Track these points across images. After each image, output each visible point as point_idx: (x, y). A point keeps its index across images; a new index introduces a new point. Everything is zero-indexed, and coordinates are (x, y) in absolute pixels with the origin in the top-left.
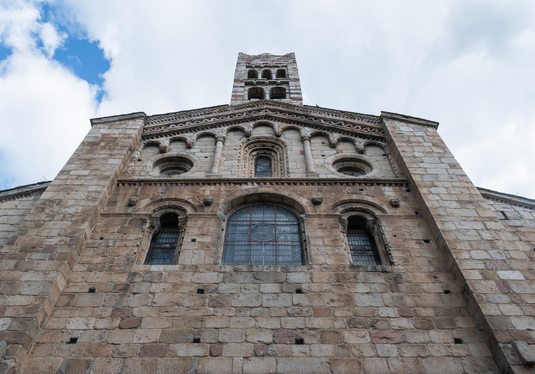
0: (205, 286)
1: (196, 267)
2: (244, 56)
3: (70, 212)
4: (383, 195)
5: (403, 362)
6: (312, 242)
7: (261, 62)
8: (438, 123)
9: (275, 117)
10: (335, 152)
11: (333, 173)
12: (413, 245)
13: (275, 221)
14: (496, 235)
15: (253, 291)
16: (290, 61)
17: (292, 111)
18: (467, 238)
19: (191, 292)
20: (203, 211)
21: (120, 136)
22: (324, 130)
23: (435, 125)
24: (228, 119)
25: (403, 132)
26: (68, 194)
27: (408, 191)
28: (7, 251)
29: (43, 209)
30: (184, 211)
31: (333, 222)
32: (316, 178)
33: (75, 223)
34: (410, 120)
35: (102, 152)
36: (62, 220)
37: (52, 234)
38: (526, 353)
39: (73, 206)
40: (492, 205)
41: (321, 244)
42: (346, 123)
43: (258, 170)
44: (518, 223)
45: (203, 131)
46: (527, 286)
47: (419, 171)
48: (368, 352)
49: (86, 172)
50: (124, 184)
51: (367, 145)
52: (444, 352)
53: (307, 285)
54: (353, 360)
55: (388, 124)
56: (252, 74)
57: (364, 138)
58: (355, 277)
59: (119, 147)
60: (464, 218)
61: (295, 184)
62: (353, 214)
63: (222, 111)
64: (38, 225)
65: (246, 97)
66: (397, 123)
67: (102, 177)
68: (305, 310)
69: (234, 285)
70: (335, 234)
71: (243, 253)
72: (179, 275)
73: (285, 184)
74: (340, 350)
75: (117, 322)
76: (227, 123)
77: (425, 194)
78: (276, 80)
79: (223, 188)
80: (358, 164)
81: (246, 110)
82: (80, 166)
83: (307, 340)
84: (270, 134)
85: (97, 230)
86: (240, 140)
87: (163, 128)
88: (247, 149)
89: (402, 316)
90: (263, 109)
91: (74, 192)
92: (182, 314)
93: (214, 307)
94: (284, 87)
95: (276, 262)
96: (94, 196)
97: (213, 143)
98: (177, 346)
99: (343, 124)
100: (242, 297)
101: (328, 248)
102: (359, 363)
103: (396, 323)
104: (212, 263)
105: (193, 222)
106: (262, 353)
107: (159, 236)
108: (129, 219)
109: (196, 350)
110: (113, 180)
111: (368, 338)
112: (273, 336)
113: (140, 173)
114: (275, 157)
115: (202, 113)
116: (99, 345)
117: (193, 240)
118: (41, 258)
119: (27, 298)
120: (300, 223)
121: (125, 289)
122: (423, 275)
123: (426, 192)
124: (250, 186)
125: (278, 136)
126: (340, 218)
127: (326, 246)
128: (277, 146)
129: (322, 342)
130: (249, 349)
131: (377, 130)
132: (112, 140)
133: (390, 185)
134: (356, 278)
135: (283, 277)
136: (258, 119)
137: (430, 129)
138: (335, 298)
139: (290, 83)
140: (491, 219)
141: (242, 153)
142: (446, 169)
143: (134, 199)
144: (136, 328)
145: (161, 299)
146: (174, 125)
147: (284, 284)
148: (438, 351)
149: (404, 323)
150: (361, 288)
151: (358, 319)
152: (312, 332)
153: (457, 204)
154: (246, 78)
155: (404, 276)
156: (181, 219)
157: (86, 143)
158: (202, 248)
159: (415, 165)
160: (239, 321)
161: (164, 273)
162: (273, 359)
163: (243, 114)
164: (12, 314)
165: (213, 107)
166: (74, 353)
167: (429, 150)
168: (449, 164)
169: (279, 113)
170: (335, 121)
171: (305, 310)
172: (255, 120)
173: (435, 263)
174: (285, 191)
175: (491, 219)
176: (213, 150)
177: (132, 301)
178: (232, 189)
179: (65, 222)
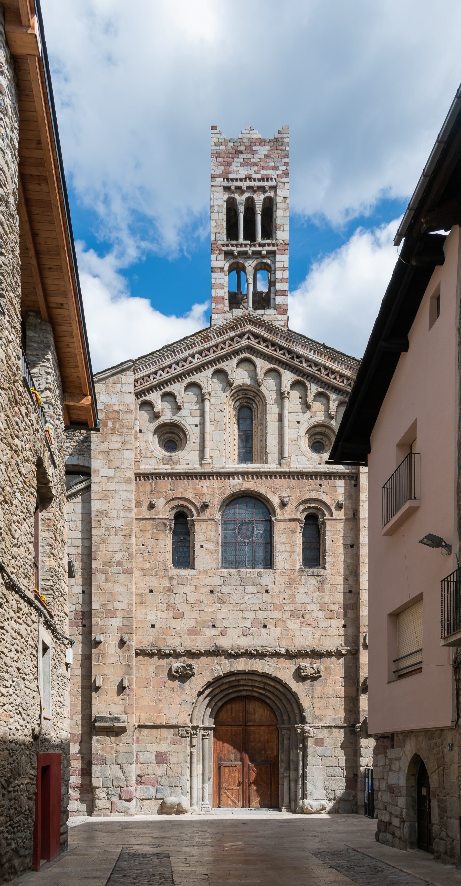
0: (214, 588)
1: (207, 572)
65: (225, 239)
69: (230, 587)
75: (171, 615)
95: (253, 546)
104: (216, 568)
121: (169, 590)
132: (116, 416)
145: (192, 598)
177: (175, 599)
178: (223, 485)
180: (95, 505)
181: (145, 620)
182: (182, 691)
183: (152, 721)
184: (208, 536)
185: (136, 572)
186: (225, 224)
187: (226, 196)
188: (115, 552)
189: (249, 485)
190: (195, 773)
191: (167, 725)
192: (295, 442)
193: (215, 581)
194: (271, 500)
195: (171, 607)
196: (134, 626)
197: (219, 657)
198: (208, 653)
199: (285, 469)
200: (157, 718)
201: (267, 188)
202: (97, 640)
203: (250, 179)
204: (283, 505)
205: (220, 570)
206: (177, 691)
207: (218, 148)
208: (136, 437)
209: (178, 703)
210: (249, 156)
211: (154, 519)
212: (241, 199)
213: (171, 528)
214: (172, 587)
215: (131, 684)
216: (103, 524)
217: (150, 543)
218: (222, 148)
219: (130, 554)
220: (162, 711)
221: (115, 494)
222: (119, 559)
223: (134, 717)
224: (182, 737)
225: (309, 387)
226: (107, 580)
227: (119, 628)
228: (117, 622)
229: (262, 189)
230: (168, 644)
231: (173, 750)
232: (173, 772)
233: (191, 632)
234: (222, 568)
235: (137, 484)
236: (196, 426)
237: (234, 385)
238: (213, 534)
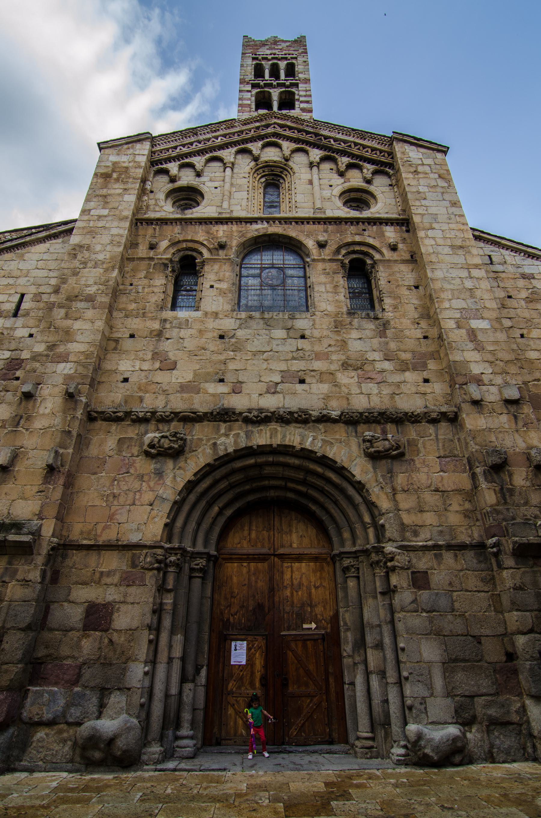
0: (225, 332)
2: (249, 42)
3: (100, 259)
4: (384, 236)
5: (381, 397)
6: (316, 288)
7: (269, 52)
8: (448, 148)
9: (283, 135)
10: (341, 180)
11: (339, 208)
12: (404, 292)
13: (284, 264)
14: (477, 283)
15: (264, 336)
16: (300, 51)
17: (301, 127)
18: (451, 287)
19: (214, 337)
20: (218, 255)
21: (131, 164)
22: (333, 153)
23: (444, 150)
24: (236, 138)
25: (412, 160)
26: (94, 238)
27: (408, 231)
28: (55, 300)
29: (75, 256)
30: (201, 253)
31: (335, 267)
32: (323, 216)
33: (106, 270)
34: (420, 143)
35: (116, 186)
36: (94, 268)
37: (89, 283)
38: (475, 393)
39: (100, 251)
40: (481, 248)
41: (324, 290)
42: (356, 144)
43: (267, 200)
44: (500, 268)
45: (211, 155)
46: (491, 334)
47: (420, 211)
48: (355, 390)
49: (105, 212)
50: (142, 223)
51: (375, 173)
52: (414, 390)
53: (310, 331)
54: (343, 397)
55: (398, 147)
56: (259, 71)
57: (373, 164)
58: (350, 323)
59: (131, 180)
60: (453, 266)
61: (303, 223)
62: (354, 256)
63: (229, 128)
64: (75, 273)
66: (407, 147)
67: (121, 217)
69: (249, 331)
70: (336, 279)
71: (256, 298)
72: (202, 321)
73: (293, 223)
74: (334, 389)
75: (157, 365)
76: (235, 143)
77: (422, 238)
79: (235, 228)
80: (364, 196)
82: (98, 203)
83: (308, 380)
84: (278, 156)
85: (126, 275)
86: (248, 165)
87: (170, 150)
88: (255, 175)
89: (386, 360)
90: (272, 124)
91: (100, 236)
92: (208, 358)
93: (233, 351)
94: (293, 90)
96: (118, 240)
97: (222, 169)
98: (207, 385)
99: (353, 146)
100: (256, 342)
101: (330, 294)
102: (348, 399)
103: (379, 366)
104: (230, 310)
105: (210, 267)
106: (273, 390)
107: (180, 279)
108: (153, 263)
109: (222, 388)
110: (132, 220)
112: (282, 377)
113: (154, 208)
114: (283, 185)
115: (209, 130)
116: (147, 384)
117: (212, 287)
118: (85, 307)
119: (83, 345)
120: (304, 267)
121: (159, 334)
122: (408, 321)
123: (424, 236)
124: (259, 226)
125: (287, 160)
126: (342, 263)
127: (328, 292)
128: (286, 173)
129: (321, 382)
130: (262, 387)
131: (386, 155)
133: (392, 224)
134: (352, 325)
135: (289, 324)
136: (267, 138)
137: (439, 155)
138: (333, 343)
139: (300, 85)
140: (476, 266)
141: (251, 182)
142: (447, 208)
143: (154, 241)
144: (173, 369)
145: (190, 344)
146: (181, 147)
147: (291, 331)
149: (387, 365)
151: (350, 362)
152: (312, 373)
153: (449, 249)
154: (253, 79)
155: (392, 323)
156: (199, 262)
157: (99, 174)
158: (220, 294)
159: (417, 203)
160: (254, 364)
161: (190, 320)
162: (281, 396)
163: (250, 131)
164: (75, 360)
165: (220, 123)
166: (128, 390)
167: (433, 183)
168: (450, 201)
169: (287, 129)
170: (345, 142)
172: (263, 139)
173: (420, 310)
174: (292, 231)
175: (476, 266)
176: (222, 178)
177: (166, 346)
178: (243, 229)
179: (98, 269)
182: (159, 480)
184: (221, 276)
190: (163, 656)
191: (120, 543)
194: (304, 242)
197: (228, 424)
199: (319, 216)
200: (104, 529)
206: (149, 481)
209: (147, 502)
214: (164, 331)
220: (118, 517)
221: (103, 231)
224: (146, 569)
230: (145, 406)
231: (122, 599)
232: (115, 651)
233: (184, 388)
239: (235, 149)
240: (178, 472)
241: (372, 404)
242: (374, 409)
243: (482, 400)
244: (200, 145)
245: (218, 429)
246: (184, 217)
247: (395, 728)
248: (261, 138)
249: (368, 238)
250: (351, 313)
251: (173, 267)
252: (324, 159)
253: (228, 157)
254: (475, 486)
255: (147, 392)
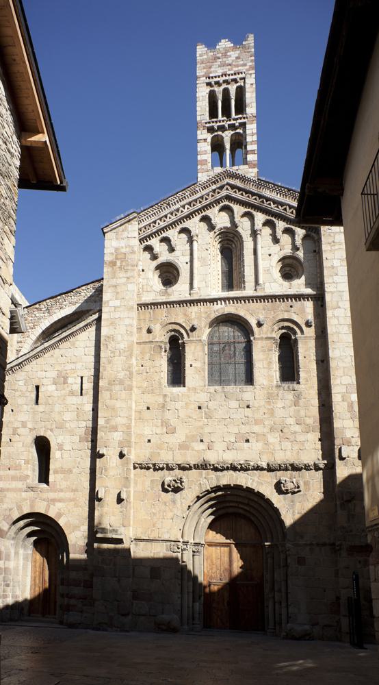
11: (275, 281)
24: (198, 206)
32: (263, 294)
41: (262, 367)
62: (284, 331)
68: (251, 420)
75: (165, 430)
78: (234, 120)
79: (201, 308)
81: (211, 190)
98: (194, 444)
100: (220, 412)
101: (266, 370)
108: (153, 346)
109: (202, 446)
111: (279, 438)
127: (264, 368)
130: (224, 446)
138: (266, 412)
145: (182, 414)
148: (309, 447)
149: (297, 428)
150: (280, 404)
152: (253, 435)
154: (208, 120)
155: (303, 394)
162: (235, 451)
163: (208, 195)
170: (282, 204)
171: (251, 420)
177: (169, 415)
180: (104, 331)
181: (142, 435)
183: (146, 535)
185: (135, 389)
186: (208, 109)
187: (208, 89)
188: (118, 372)
189: (230, 309)
192: (267, 271)
193: (202, 397)
194: (250, 321)
195: (165, 423)
196: (133, 440)
198: (197, 467)
201: (238, 80)
202: (100, 452)
203: (226, 76)
204: (259, 325)
205: (207, 387)
207: (202, 58)
208: (139, 275)
210: (224, 59)
211: (151, 342)
212: (219, 91)
213: (165, 351)
215: (128, 496)
216: (109, 347)
217: (148, 364)
218: (205, 57)
219: (131, 373)
222: (121, 377)
223: (131, 530)
225: (277, 225)
226: (111, 398)
227: (120, 443)
228: (117, 436)
229: (235, 81)
234: (209, 386)
235: (138, 313)
236: (187, 263)
237: (217, 228)
238: (201, 353)
239: (199, 217)
240: (183, 501)
241: (287, 457)
242: (287, 460)
243: (348, 457)
244: (173, 217)
245: (202, 475)
246: (168, 300)
247: (283, 625)
248: (218, 202)
249: (293, 314)
250: (278, 386)
251: (165, 348)
252: (265, 224)
253: (194, 228)
254: (336, 512)
255: (161, 449)
